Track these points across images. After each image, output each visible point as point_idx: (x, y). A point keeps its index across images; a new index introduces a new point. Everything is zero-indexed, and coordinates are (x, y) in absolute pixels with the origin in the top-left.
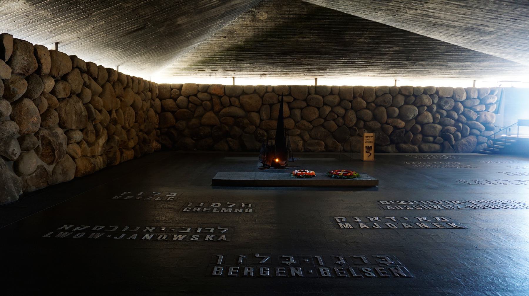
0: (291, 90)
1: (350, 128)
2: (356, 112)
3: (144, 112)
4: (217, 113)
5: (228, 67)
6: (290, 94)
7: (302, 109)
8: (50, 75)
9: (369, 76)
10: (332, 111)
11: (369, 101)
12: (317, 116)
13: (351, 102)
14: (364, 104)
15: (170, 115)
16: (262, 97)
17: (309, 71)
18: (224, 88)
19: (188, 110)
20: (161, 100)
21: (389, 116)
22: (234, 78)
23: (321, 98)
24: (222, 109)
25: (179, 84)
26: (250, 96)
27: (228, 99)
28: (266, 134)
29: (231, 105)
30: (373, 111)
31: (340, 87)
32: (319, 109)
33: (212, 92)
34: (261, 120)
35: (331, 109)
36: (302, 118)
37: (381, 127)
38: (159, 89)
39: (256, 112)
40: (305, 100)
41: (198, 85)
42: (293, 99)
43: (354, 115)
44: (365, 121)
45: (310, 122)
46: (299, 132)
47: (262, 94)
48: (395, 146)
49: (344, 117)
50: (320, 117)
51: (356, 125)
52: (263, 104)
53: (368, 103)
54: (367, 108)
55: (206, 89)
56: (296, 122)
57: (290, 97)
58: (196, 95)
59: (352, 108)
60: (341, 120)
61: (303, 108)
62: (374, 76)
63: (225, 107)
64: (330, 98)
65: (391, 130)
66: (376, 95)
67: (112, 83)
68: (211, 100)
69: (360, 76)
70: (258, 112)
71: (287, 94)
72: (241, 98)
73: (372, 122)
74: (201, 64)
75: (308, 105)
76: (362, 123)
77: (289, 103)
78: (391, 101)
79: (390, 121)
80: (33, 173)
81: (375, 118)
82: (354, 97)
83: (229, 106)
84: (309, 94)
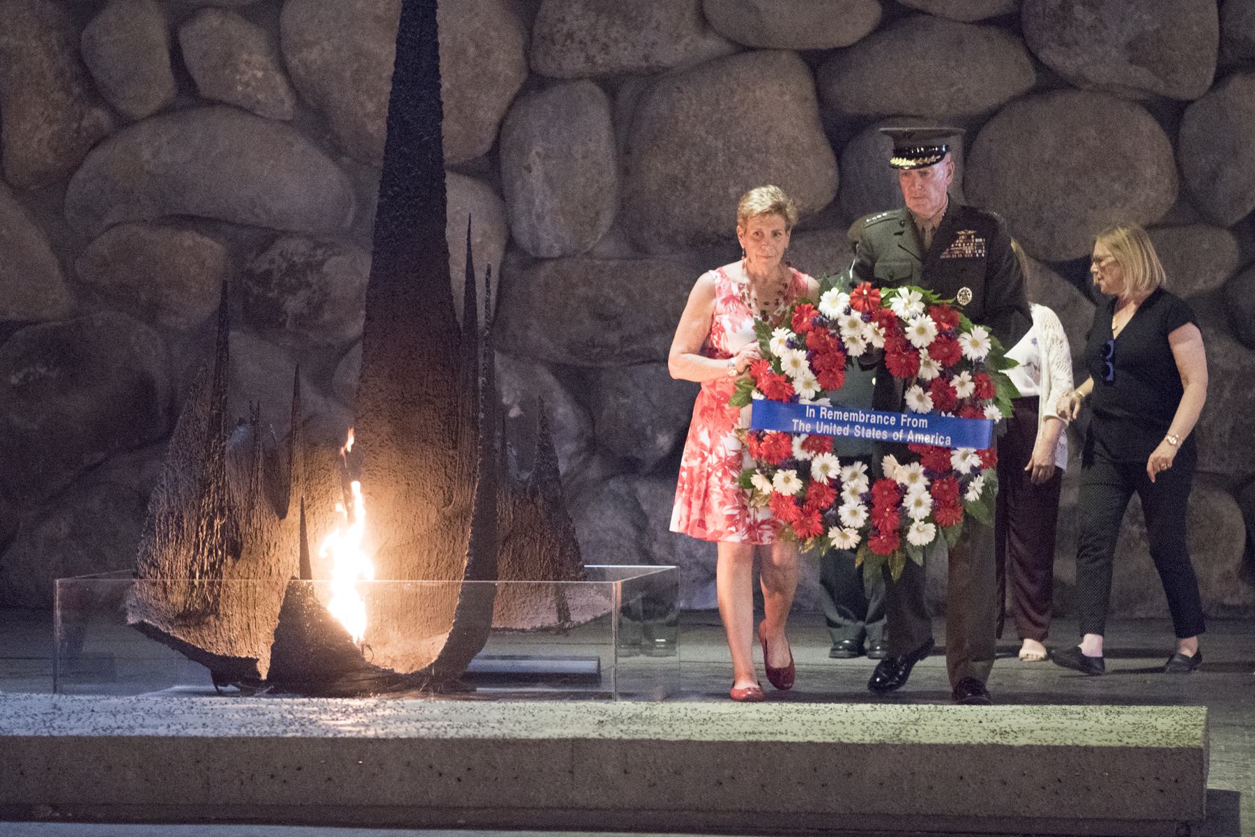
7: (973, 128)
24: (99, 140)
27: (157, 33)
28: (564, 411)
29: (189, 93)
32: (1170, 114)
40: (1010, 24)
52: (536, 83)
61: (993, 113)
63: (124, 122)
75: (1050, 83)
77: (820, 63)
83: (165, 111)
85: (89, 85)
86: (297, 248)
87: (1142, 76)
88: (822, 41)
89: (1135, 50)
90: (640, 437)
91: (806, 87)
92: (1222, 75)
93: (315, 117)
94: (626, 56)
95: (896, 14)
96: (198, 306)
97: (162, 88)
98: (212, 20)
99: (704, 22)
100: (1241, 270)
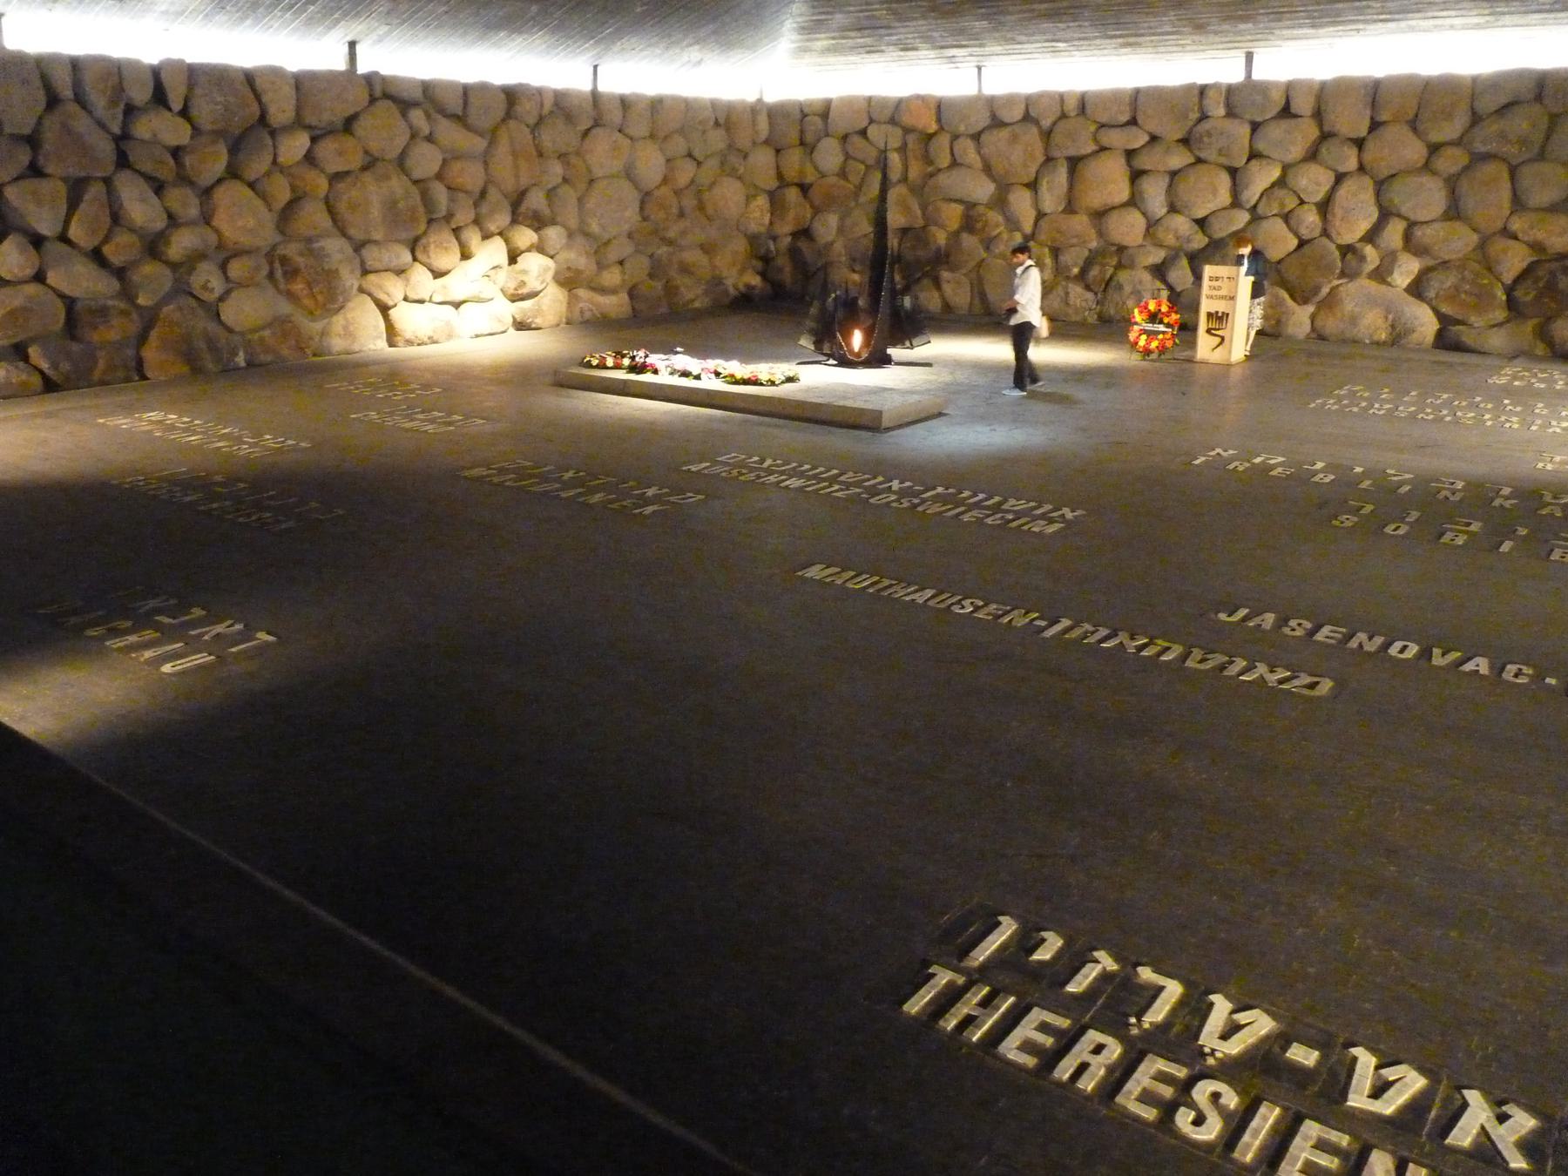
0: (1136, 106)
1: (1346, 250)
2: (1380, 186)
3: (678, 193)
4: (918, 190)
5: (935, 34)
6: (1133, 122)
7: (1173, 174)
8: (299, 123)
9: (1452, 27)
10: (1281, 183)
11: (1436, 137)
12: (1224, 197)
13: (1359, 143)
14: (1414, 151)
15: (793, 194)
16: (1047, 135)
17: (1200, 28)
18: (940, 107)
19: (842, 182)
20: (778, 151)
21: (1518, 204)
22: (979, 68)
23: (1246, 130)
24: (931, 175)
25: (818, 101)
26: (1009, 129)
29: (955, 164)
30: (1452, 184)
31: (1323, 86)
32: (1233, 172)
33: (907, 120)
34: (1040, 215)
35: (1276, 173)
36: (1173, 209)
37: (1482, 246)
38: (769, 116)
39: (1027, 185)
40: (1185, 142)
41: (869, 100)
42: (1146, 138)
43: (1368, 196)
44: (1412, 225)
45: (1201, 223)
46: (1157, 256)
47: (1046, 123)
48: (1530, 325)
49: (1324, 207)
50: (1236, 203)
51: (1371, 237)
52: (1049, 160)
53: (1434, 149)
54: (1427, 167)
55: (894, 113)
56: (1152, 225)
57: (1134, 128)
58: (863, 133)
59: (1362, 168)
60: (1310, 219)
61: (1180, 171)
62: (1477, 26)
64: (1276, 131)
65: (1514, 260)
66: (1474, 113)
67: (532, 121)
68: (903, 149)
69: (1412, 29)
70: (1033, 186)
71: (1124, 118)
72: (984, 137)
73: (1436, 226)
74: (853, 34)
75: (1199, 161)
76: (1394, 233)
77: (1130, 154)
78: (1538, 137)
79: (1516, 225)
80: (263, 328)
81: (1454, 212)
82: (1375, 126)
84: (1204, 117)
85: (927, 159)
86: (981, 209)
87: (1223, 160)
88: (1131, 147)
89: (1220, 152)
90: (1068, 269)
91: (1123, 161)
92: (1249, 160)
93: (988, 169)
94: (1072, 152)
95: (1154, 139)
96: (954, 225)
97: (944, 161)
98: (961, 140)
99: (1096, 140)
100: (1249, 223)
